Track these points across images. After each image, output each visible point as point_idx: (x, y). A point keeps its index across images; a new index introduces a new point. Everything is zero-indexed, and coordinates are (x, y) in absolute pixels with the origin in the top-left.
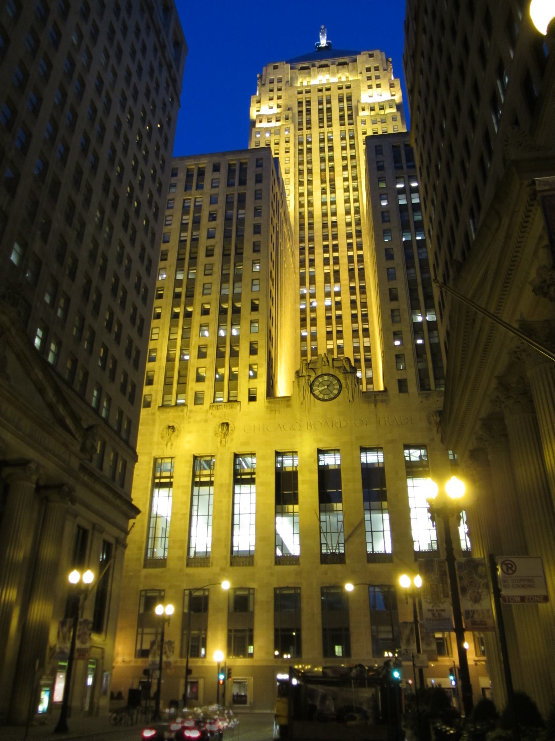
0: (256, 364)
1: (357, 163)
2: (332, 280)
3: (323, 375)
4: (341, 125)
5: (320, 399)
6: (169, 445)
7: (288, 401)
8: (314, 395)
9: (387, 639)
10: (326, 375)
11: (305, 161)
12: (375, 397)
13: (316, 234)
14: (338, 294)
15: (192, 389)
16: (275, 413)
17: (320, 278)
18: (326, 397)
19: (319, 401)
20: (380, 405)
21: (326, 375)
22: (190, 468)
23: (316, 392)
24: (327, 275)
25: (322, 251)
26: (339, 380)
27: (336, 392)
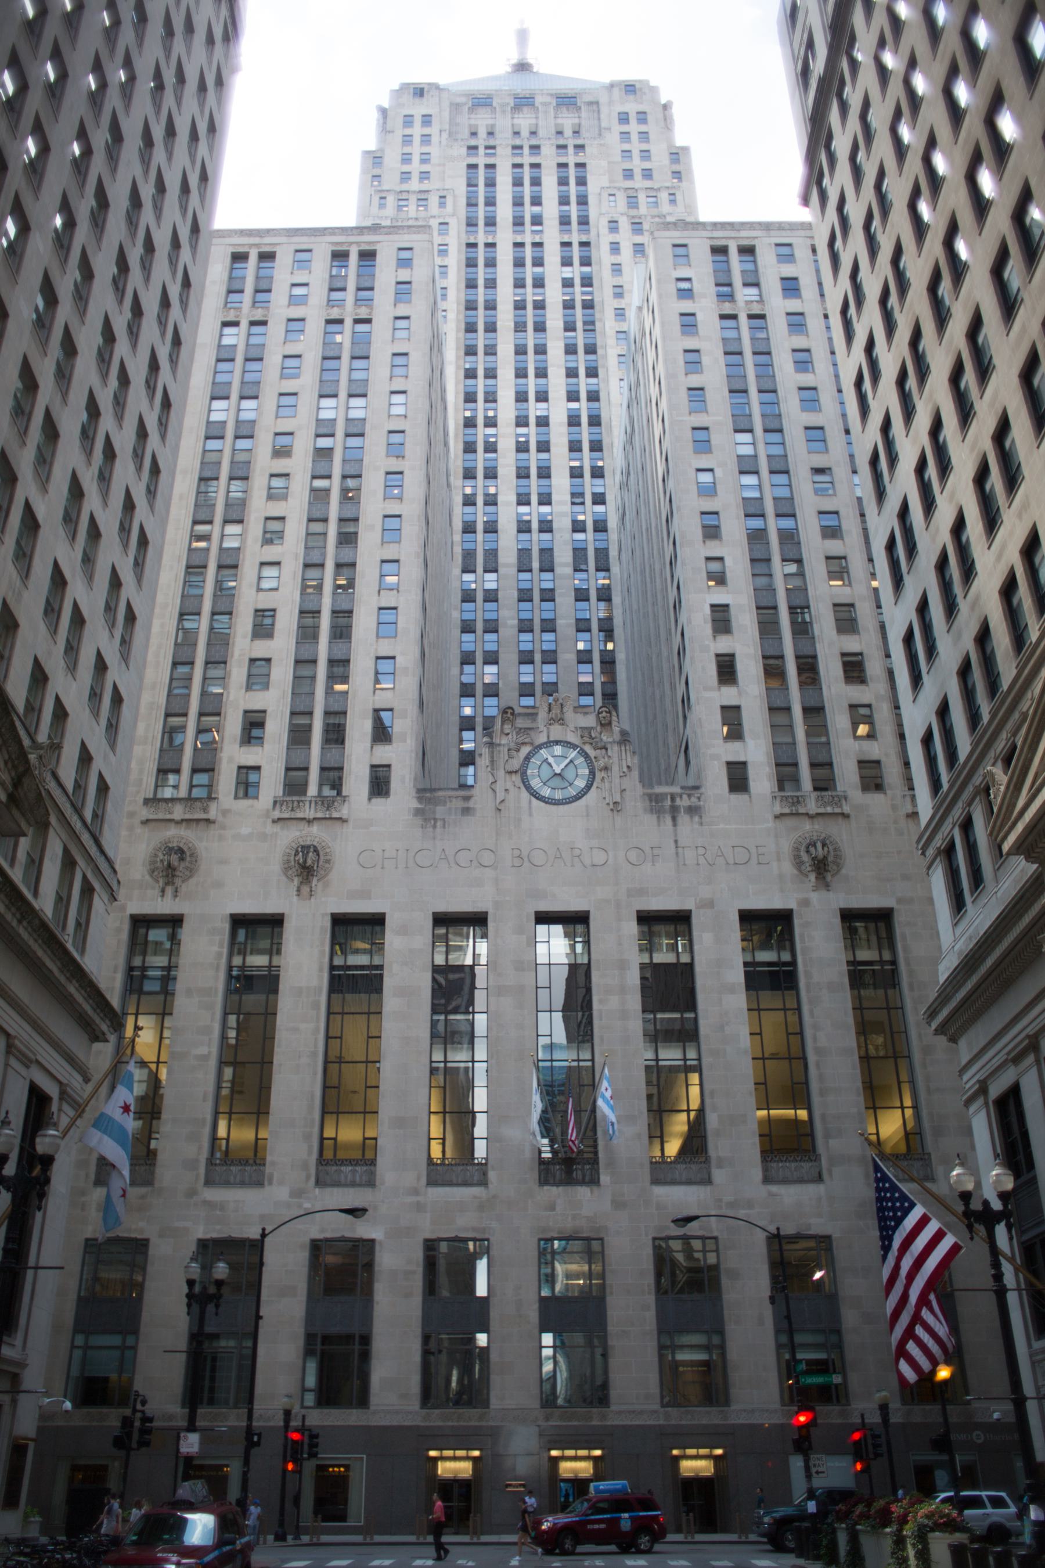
0: (391, 710)
1: (597, 316)
2: (536, 565)
3: (550, 744)
6: (169, 890)
7: (467, 798)
8: (528, 788)
12: (673, 799)
13: (501, 462)
14: (548, 596)
15: (231, 760)
16: (435, 827)
17: (508, 557)
18: (558, 795)
19: (542, 804)
20: (683, 818)
21: (557, 742)
22: (221, 946)
23: (535, 783)
24: (524, 554)
25: (513, 498)
26: (586, 756)
27: (581, 783)
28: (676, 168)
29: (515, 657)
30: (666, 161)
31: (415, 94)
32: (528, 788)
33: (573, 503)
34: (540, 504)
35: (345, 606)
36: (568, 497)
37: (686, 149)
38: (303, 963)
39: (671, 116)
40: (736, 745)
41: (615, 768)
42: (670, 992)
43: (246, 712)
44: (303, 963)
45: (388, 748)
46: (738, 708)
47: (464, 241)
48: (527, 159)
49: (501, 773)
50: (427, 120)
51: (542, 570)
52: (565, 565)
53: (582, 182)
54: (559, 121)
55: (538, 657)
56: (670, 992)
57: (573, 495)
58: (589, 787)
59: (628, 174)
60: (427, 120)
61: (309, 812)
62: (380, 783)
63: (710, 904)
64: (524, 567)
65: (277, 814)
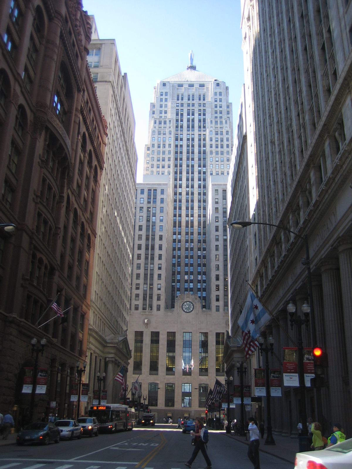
1: (206, 157)
2: (190, 226)
4: (199, 131)
5: (185, 312)
8: (183, 310)
9: (204, 402)
10: (188, 301)
11: (179, 152)
17: (184, 224)
18: (188, 311)
21: (188, 301)
23: (184, 309)
24: (187, 222)
25: (185, 208)
26: (193, 304)
27: (192, 309)
28: (228, 110)
29: (184, 249)
30: (226, 108)
31: (163, 86)
32: (183, 310)
33: (198, 210)
34: (191, 217)
35: (152, 273)
36: (197, 208)
37: (231, 103)
38: (147, 339)
39: (228, 92)
40: (218, 302)
41: (197, 307)
42: (204, 345)
43: (136, 294)
44: (147, 339)
45: (160, 301)
46: (219, 295)
47: (175, 133)
48: (191, 108)
49: (179, 307)
50: (166, 94)
51: (191, 227)
52: (196, 226)
53: (204, 115)
54: (200, 92)
55: (189, 249)
56: (204, 345)
57: (199, 207)
58: (193, 310)
59: (216, 113)
60: (166, 94)
61: (147, 313)
62: (158, 309)
63: (211, 331)
64: (187, 226)
65: (142, 314)
